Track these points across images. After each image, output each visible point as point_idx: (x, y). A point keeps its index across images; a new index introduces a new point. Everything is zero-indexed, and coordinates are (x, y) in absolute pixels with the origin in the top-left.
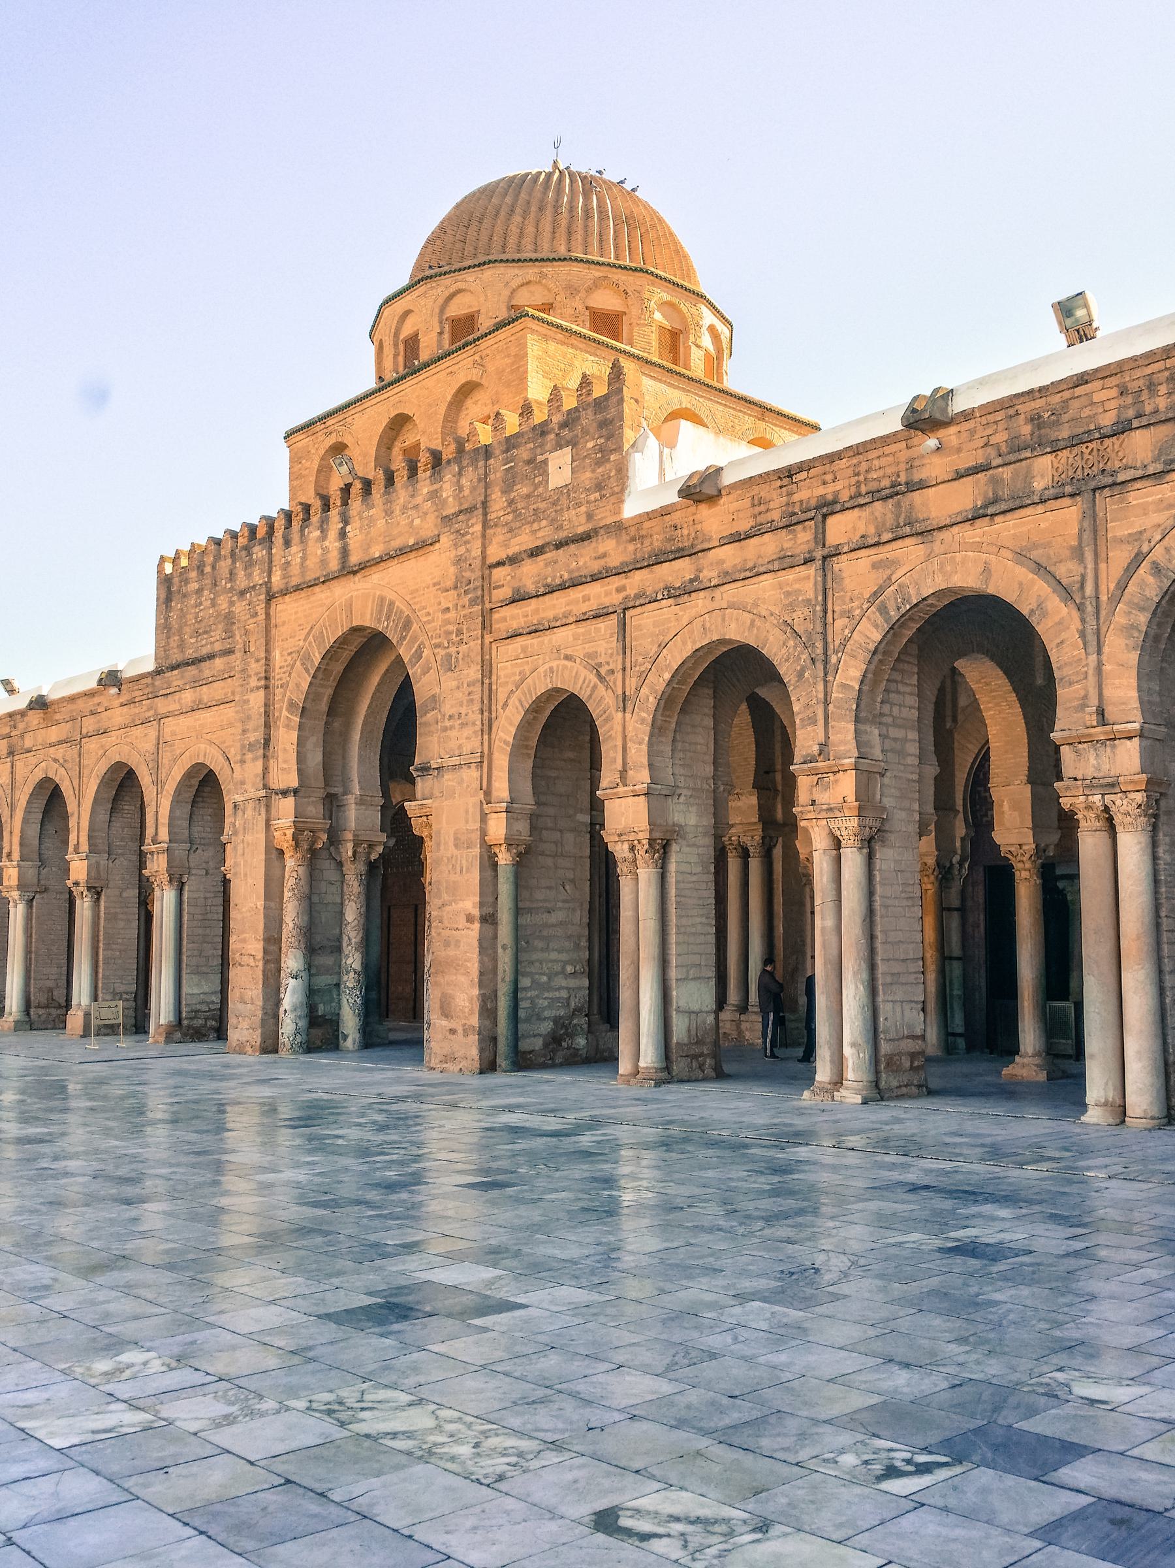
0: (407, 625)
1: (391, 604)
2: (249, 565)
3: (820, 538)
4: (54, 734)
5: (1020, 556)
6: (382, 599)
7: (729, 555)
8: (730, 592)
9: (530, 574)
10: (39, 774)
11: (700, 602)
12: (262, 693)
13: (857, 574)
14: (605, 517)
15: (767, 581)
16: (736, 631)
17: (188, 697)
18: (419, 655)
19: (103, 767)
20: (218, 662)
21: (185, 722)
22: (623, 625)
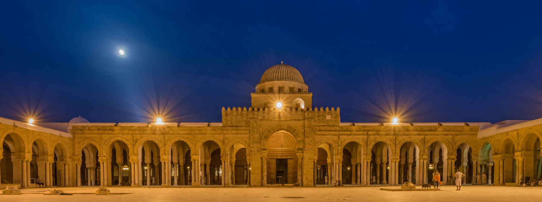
0: (295, 130)
1: (291, 127)
2: (253, 114)
3: (368, 133)
4: (183, 132)
5: (390, 139)
6: (289, 126)
7: (356, 132)
8: (356, 136)
9: (322, 128)
10: (177, 139)
11: (351, 136)
12: (258, 135)
13: (372, 137)
14: (336, 124)
15: (361, 136)
16: (356, 140)
17: (234, 132)
18: (298, 134)
19: (204, 141)
20: (244, 128)
21: (232, 136)
22: (339, 137)
